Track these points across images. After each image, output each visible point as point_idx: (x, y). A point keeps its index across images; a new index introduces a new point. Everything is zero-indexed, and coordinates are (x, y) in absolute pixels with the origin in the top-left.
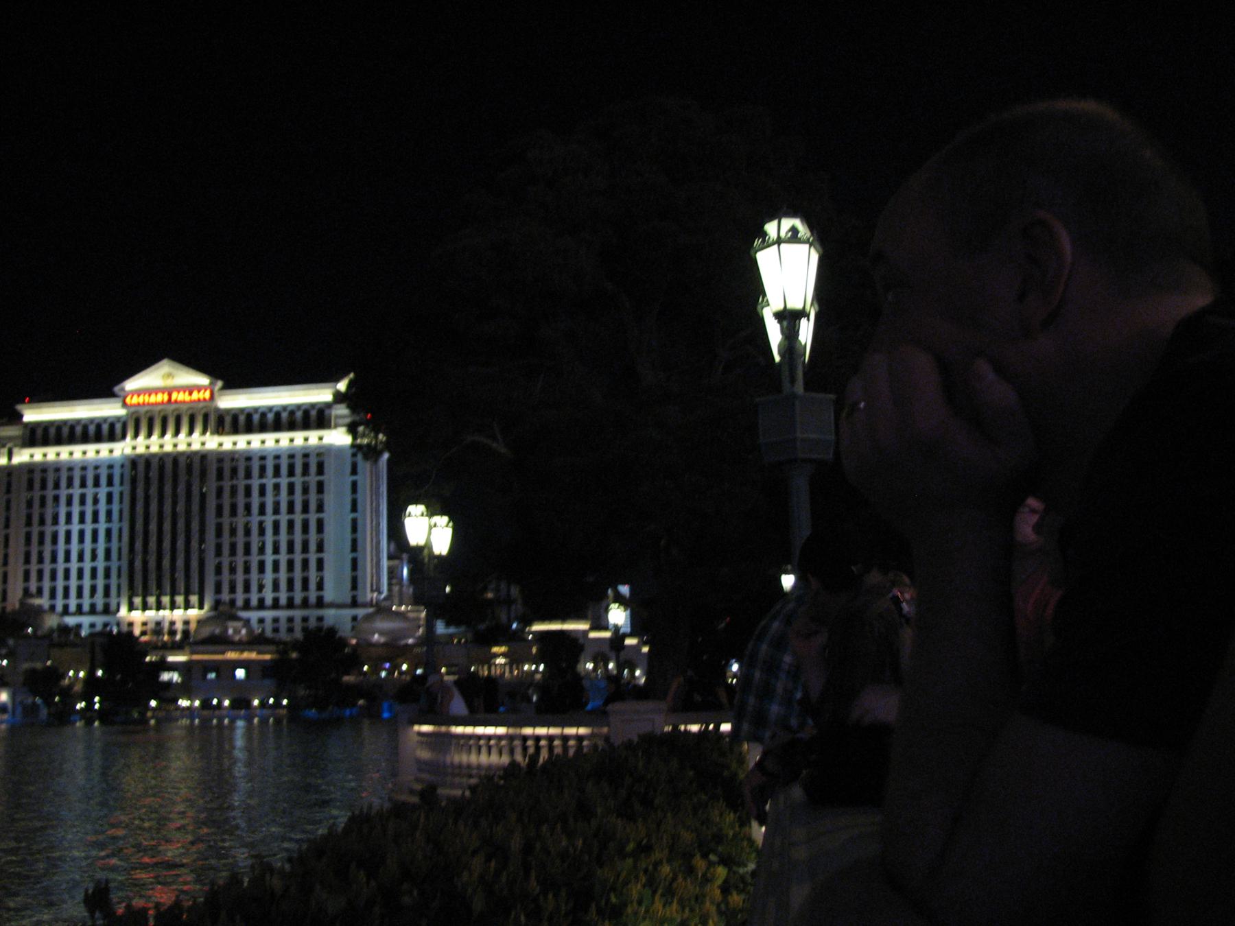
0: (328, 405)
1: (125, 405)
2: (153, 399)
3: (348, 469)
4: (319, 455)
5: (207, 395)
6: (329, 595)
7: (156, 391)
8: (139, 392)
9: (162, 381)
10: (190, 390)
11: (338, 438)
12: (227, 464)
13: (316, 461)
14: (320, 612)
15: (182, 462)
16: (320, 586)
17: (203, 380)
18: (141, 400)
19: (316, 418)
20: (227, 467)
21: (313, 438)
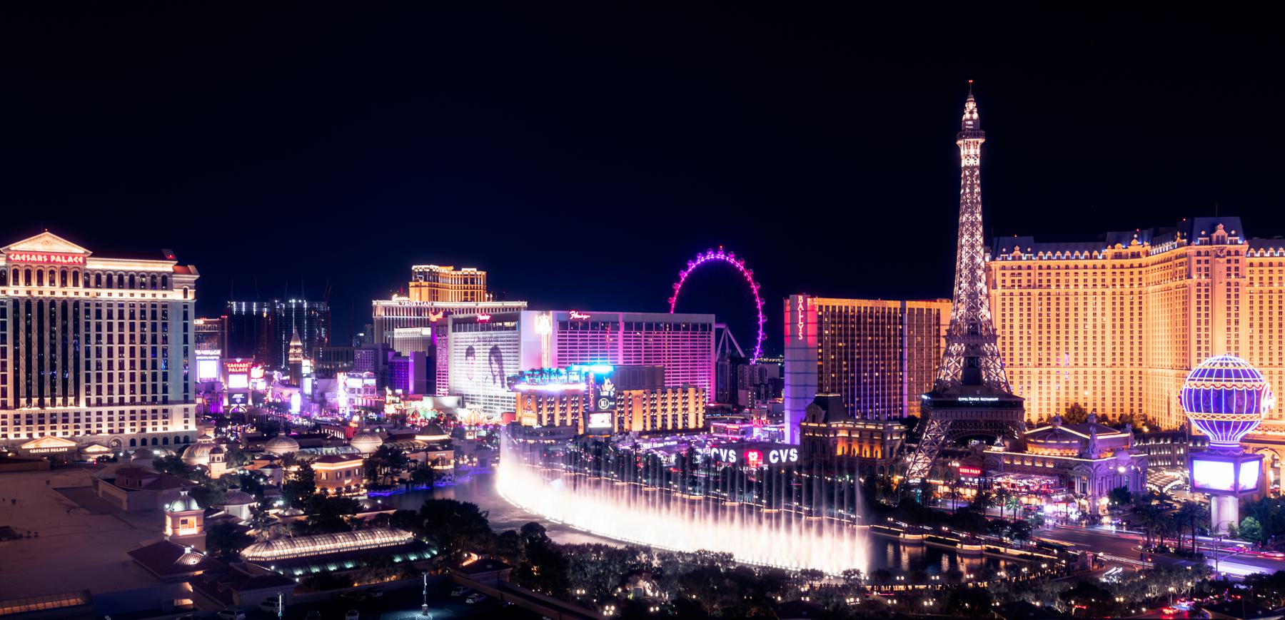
0: (170, 274)
1: (8, 259)
2: (34, 258)
3: (182, 316)
4: (165, 306)
5: (81, 260)
6: (171, 397)
7: (36, 253)
8: (21, 253)
9: (46, 246)
10: (66, 255)
11: (175, 295)
12: (71, 310)
13: (158, 313)
14: (165, 407)
15: (59, 305)
16: (165, 390)
17: (80, 250)
18: (23, 257)
19: (163, 282)
20: (93, 309)
21: (159, 295)
